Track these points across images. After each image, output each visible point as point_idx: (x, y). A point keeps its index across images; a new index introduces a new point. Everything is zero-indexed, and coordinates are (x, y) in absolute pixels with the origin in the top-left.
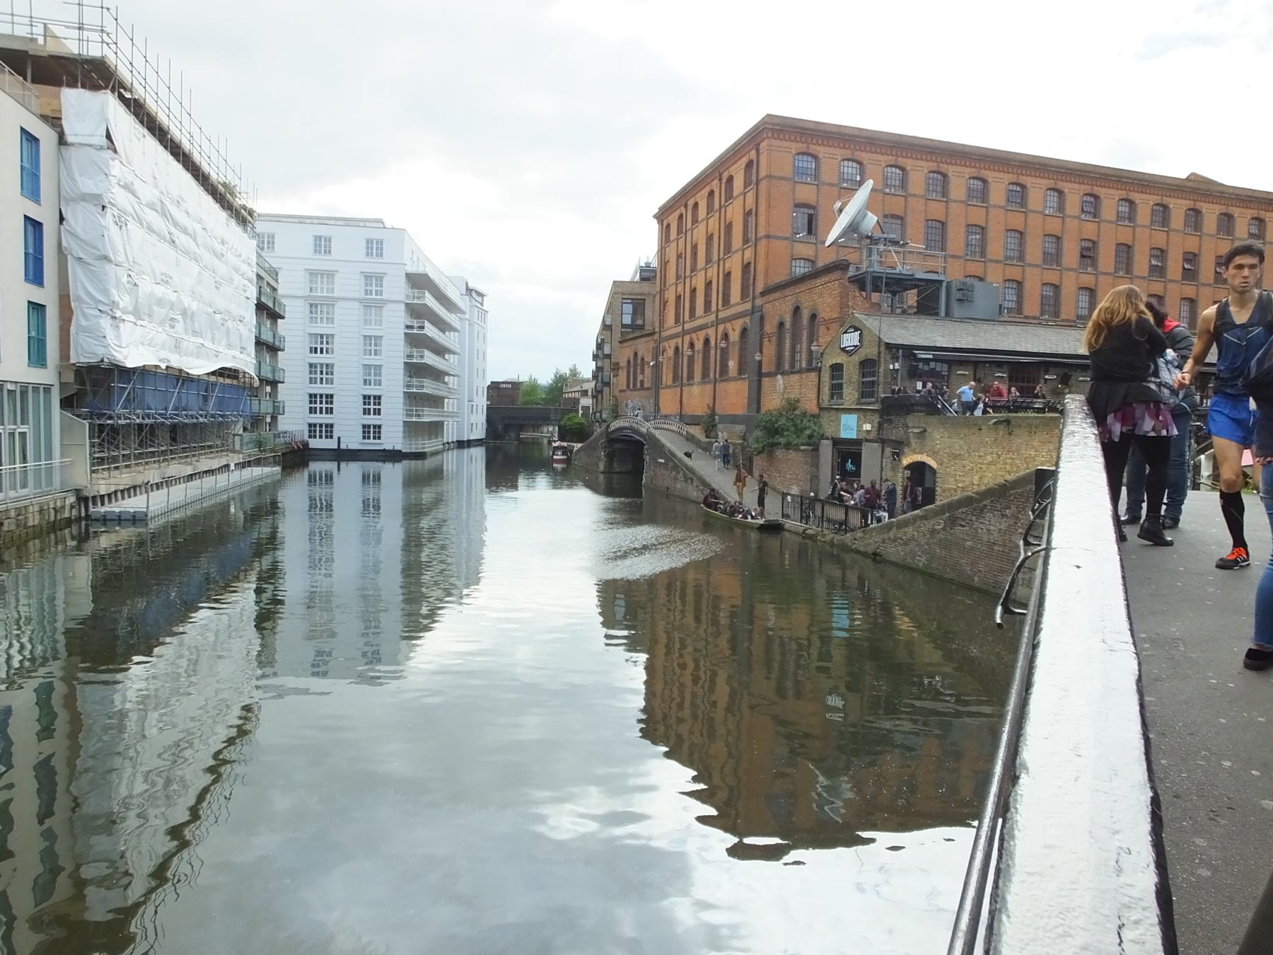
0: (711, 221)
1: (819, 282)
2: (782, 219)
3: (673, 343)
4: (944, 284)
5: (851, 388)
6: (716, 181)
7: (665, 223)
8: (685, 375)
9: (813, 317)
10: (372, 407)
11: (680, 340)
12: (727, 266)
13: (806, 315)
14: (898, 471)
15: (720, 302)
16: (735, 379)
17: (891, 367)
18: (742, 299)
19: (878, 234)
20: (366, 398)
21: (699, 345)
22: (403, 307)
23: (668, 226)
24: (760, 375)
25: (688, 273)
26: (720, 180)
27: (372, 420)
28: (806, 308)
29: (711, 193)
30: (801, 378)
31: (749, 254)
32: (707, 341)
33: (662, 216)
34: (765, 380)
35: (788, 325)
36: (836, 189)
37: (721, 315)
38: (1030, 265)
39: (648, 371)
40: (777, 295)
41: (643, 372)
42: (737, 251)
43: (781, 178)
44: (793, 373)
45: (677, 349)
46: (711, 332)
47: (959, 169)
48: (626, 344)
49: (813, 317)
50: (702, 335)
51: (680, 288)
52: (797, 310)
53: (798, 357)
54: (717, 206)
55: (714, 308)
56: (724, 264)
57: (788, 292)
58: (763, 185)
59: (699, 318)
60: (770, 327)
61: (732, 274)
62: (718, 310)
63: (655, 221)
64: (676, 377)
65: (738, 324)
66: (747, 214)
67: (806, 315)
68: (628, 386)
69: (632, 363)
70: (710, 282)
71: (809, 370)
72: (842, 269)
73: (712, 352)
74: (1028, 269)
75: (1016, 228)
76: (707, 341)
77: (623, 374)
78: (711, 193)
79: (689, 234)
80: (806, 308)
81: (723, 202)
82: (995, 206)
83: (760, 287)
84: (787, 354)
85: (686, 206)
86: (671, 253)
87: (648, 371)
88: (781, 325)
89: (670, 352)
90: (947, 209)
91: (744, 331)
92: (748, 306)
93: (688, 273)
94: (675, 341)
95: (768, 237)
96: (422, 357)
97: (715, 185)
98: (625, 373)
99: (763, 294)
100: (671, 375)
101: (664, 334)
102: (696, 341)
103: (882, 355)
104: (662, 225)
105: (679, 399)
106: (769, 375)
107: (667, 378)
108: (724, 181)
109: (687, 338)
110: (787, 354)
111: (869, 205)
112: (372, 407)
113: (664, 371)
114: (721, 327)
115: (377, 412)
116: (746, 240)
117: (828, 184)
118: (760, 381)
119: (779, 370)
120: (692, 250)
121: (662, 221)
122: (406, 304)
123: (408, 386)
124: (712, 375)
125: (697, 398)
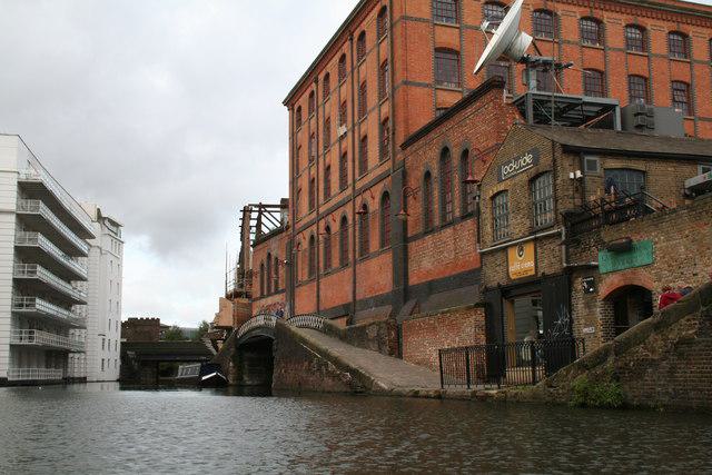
0: (344, 88)
1: (469, 110)
2: (422, 65)
3: (307, 234)
4: (618, 109)
6: (348, 43)
7: (296, 107)
8: (322, 265)
11: (315, 227)
12: (362, 130)
13: (456, 153)
14: (595, 306)
15: (357, 171)
16: (378, 254)
17: (572, 176)
18: (381, 159)
19: (534, 57)
21: (335, 227)
22: (13, 218)
23: (300, 109)
24: (406, 240)
25: (321, 151)
26: (352, 39)
28: (456, 146)
29: (343, 58)
30: (455, 229)
31: (386, 109)
32: (344, 219)
33: (290, 102)
34: (412, 245)
35: (435, 173)
37: (359, 185)
38: (700, 119)
39: (282, 271)
41: (277, 273)
42: (373, 109)
44: (443, 227)
45: (312, 237)
46: (348, 210)
47: (614, 15)
48: (261, 246)
49: (465, 153)
50: (338, 215)
51: (313, 171)
52: (445, 152)
53: (449, 208)
54: (349, 69)
55: (350, 181)
56: (359, 129)
57: (432, 135)
58: (398, 29)
59: (335, 196)
60: (415, 181)
61: (369, 136)
62: (354, 182)
64: (312, 269)
65: (378, 191)
66: (382, 67)
67: (456, 153)
70: (346, 153)
71: (464, 217)
72: (497, 86)
73: (350, 230)
74: (699, 123)
75: (681, 79)
76: (344, 219)
77: (256, 282)
78: (343, 58)
79: (321, 110)
80: (456, 146)
81: (355, 63)
82: (656, 56)
83: (401, 139)
84: (436, 207)
85: (317, 82)
86: (303, 137)
87: (282, 271)
88: (428, 175)
89: (305, 244)
90: (605, 57)
91: (386, 196)
92: (388, 166)
93: (321, 151)
94: (309, 230)
95: (406, 83)
96: (35, 272)
97: (346, 48)
98: (259, 279)
99: (404, 146)
100: (306, 270)
101: (298, 226)
102: (332, 223)
103: (559, 161)
104: (293, 109)
105: (315, 294)
106: (416, 238)
107: (303, 272)
108: (356, 39)
109: (322, 223)
110: (436, 207)
111: (520, 26)
113: (300, 263)
114: (359, 201)
116: (382, 94)
117: (471, 27)
118: (405, 249)
119: (429, 230)
120: (325, 126)
121: (293, 105)
122: (18, 215)
123: (21, 306)
124: (350, 256)
125: (337, 290)
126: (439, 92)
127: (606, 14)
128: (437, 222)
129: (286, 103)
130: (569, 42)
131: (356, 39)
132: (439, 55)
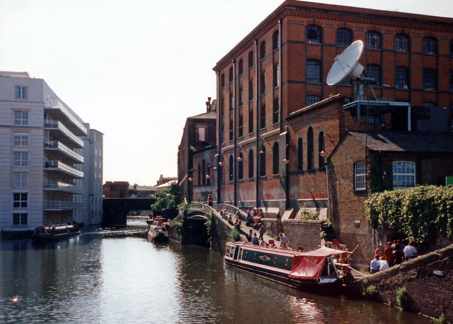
5: (349, 181)
7: (221, 73)
9: (321, 134)
10: (20, 201)
20: (16, 196)
23: (223, 75)
27: (20, 211)
36: (335, 48)
40: (298, 119)
43: (297, 42)
49: (321, 134)
55: (255, 130)
63: (215, 72)
68: (199, 183)
69: (201, 167)
76: (251, 152)
85: (235, 62)
98: (197, 174)
112: (20, 201)
115: (25, 205)
126: (308, 86)
127: (412, 31)
128: (305, 168)
129: (214, 69)
130: (387, 50)
131: (259, 44)
132: (309, 63)
